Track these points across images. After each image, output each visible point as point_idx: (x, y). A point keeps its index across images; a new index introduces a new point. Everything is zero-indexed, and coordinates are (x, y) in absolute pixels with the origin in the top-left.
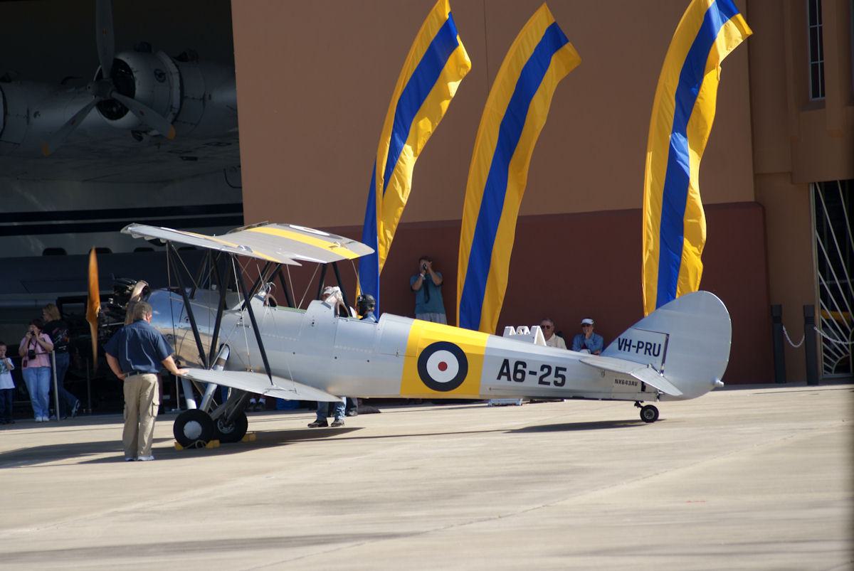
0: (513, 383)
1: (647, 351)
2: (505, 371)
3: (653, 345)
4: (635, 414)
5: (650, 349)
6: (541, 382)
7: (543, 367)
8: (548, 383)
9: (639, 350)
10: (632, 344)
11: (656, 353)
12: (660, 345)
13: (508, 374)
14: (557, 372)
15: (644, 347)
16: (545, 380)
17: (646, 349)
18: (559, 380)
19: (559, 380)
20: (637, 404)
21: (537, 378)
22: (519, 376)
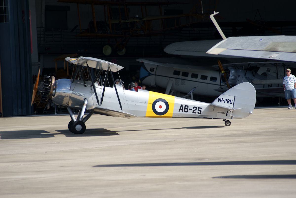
0: (184, 113)
1: (228, 102)
2: (181, 109)
3: (230, 100)
4: (223, 124)
5: (229, 101)
6: (193, 112)
7: (194, 107)
8: (196, 113)
9: (225, 102)
10: (223, 100)
11: (231, 103)
12: (232, 100)
13: (182, 110)
14: (198, 109)
15: (227, 101)
16: (195, 112)
17: (228, 101)
18: (199, 112)
19: (199, 112)
20: (224, 120)
21: (192, 111)
22: (186, 110)
